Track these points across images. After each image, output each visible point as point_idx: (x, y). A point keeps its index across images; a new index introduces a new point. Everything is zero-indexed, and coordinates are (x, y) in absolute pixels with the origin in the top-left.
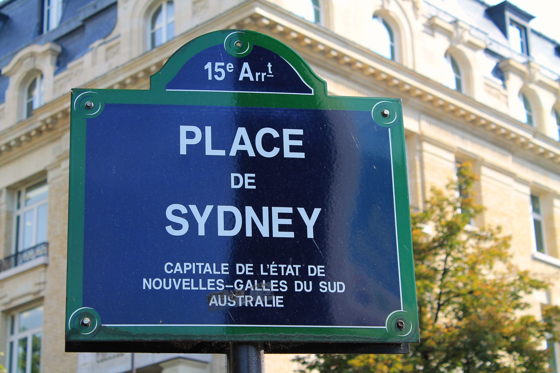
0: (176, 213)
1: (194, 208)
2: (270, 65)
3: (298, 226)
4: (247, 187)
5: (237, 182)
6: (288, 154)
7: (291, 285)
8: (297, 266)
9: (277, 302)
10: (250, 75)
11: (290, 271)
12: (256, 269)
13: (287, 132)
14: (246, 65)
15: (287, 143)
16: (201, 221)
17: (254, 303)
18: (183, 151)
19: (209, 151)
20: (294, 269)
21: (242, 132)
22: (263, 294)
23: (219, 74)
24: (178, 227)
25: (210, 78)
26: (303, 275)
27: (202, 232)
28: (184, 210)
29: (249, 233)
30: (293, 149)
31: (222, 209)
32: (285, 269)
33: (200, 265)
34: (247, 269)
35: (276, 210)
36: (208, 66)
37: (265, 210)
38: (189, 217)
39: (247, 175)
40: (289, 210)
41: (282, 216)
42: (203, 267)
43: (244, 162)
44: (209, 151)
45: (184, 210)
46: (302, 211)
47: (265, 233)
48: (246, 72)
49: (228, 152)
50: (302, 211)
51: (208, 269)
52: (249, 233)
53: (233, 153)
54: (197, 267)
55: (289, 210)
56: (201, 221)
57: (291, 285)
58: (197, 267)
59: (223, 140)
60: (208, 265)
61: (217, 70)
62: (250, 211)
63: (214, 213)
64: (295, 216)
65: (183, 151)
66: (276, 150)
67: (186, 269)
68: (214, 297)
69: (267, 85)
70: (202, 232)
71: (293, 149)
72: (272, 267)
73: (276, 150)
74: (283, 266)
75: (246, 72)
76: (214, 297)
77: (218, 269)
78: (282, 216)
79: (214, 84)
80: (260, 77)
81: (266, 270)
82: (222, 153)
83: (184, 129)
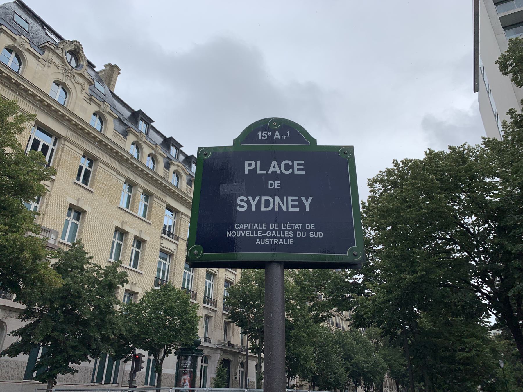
0: (242, 200)
1: (250, 198)
2: (288, 132)
3: (301, 205)
4: (276, 187)
5: (271, 186)
6: (296, 172)
8: (300, 225)
9: (290, 242)
10: (279, 137)
11: (297, 227)
12: (280, 226)
13: (296, 162)
14: (277, 132)
15: (296, 167)
16: (254, 204)
17: (278, 242)
18: (246, 172)
19: (259, 172)
20: (299, 226)
21: (274, 163)
22: (283, 238)
23: (264, 137)
24: (242, 207)
25: (260, 138)
26: (303, 229)
27: (254, 209)
28: (245, 199)
29: (277, 209)
30: (299, 170)
31: (264, 198)
32: (295, 226)
33: (252, 224)
34: (275, 226)
35: (290, 198)
36: (260, 133)
37: (285, 198)
38: (248, 202)
39: (276, 182)
40: (297, 198)
41: (293, 201)
42: (254, 226)
43: (275, 176)
44: (259, 172)
45: (245, 199)
46: (303, 198)
47: (285, 209)
48: (277, 135)
49: (267, 172)
50: (303, 198)
51: (256, 226)
52: (277, 209)
53: (270, 172)
54: (251, 226)
55: (297, 198)
56: (254, 204)
58: (251, 226)
59: (265, 166)
60: (256, 224)
61: (263, 135)
62: (277, 199)
63: (260, 200)
64: (300, 201)
65: (246, 172)
66: (291, 171)
67: (245, 226)
68: (258, 240)
69: (287, 141)
70: (254, 209)
71: (299, 170)
72: (288, 225)
73: (291, 171)
74: (293, 225)
75: (277, 135)
76: (258, 240)
77: (261, 226)
78: (293, 201)
79: (262, 141)
80: (283, 137)
81: (285, 226)
82: (265, 172)
83: (247, 162)
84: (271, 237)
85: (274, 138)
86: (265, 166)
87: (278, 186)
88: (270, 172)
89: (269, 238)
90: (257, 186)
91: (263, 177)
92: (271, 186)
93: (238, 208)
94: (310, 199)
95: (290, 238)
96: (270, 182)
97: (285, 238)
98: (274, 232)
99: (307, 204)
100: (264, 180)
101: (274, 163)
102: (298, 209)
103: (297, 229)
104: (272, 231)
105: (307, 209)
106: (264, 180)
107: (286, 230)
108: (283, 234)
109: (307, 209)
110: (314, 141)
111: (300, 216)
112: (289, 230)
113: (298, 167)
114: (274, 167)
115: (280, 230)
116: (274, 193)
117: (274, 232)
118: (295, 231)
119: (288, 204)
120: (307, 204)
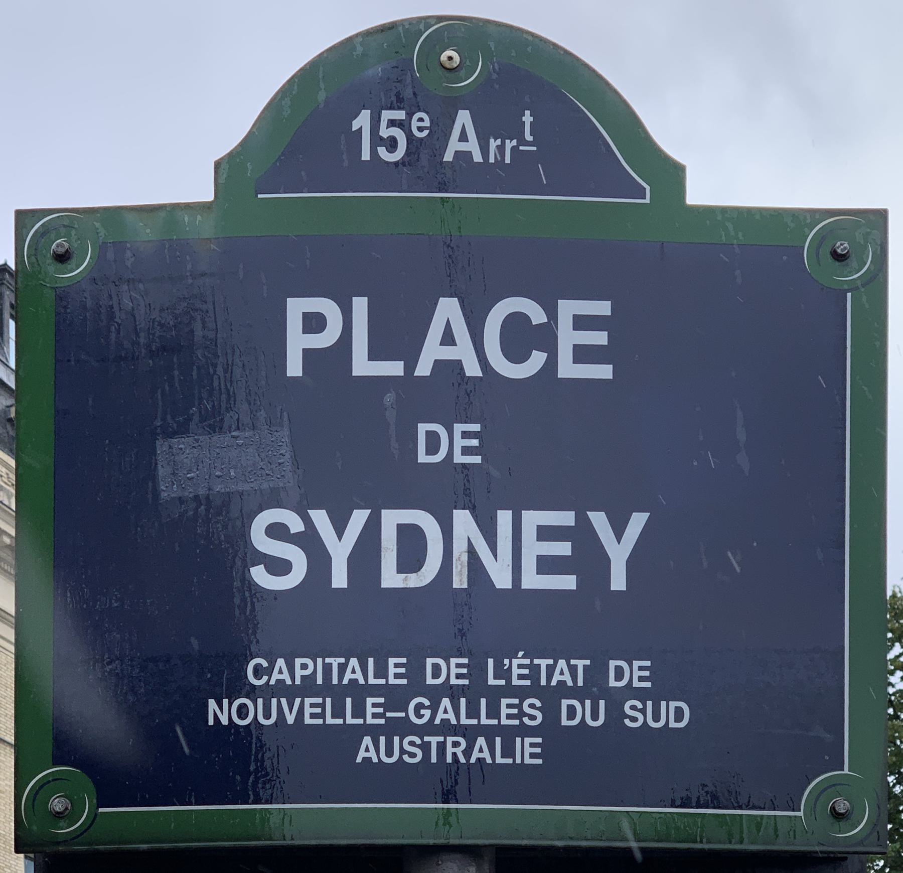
0: (277, 531)
1: (320, 518)
2: (528, 118)
3: (588, 558)
4: (459, 458)
5: (432, 449)
6: (568, 369)
7: (551, 711)
8: (580, 664)
10: (473, 146)
11: (562, 674)
12: (476, 671)
13: (567, 309)
15: (568, 338)
16: (340, 551)
18: (294, 368)
19: (362, 365)
20: (573, 670)
21: (448, 310)
22: (489, 733)
24: (280, 567)
26: (594, 687)
27: (340, 579)
28: (296, 525)
30: (582, 354)
32: (551, 670)
33: (335, 662)
35: (532, 519)
37: (504, 518)
38: (309, 541)
39: (459, 428)
40: (567, 518)
41: (545, 533)
43: (452, 392)
44: (362, 365)
45: (296, 525)
46: (599, 520)
48: (463, 137)
49: (410, 367)
50: (599, 520)
53: (423, 369)
54: (327, 668)
55: (567, 518)
56: (340, 551)
57: (551, 711)
58: (327, 668)
59: (397, 335)
63: (373, 528)
64: (582, 535)
65: (294, 368)
66: (538, 359)
67: (299, 673)
69: (516, 175)
70: (340, 579)
71: (582, 354)
72: (517, 665)
73: (538, 359)
74: (543, 663)
75: (464, 139)
78: (545, 533)
80: (501, 149)
81: (503, 673)
82: (394, 368)
83: (297, 308)
84: (430, 728)
85: (448, 157)
86: (397, 335)
87: (466, 451)
88: (423, 369)
89: (421, 731)
90: (354, 447)
91: (389, 399)
92: (432, 449)
93: (259, 575)
94: (638, 521)
95: (525, 731)
96: (423, 428)
97: (500, 730)
98: (446, 702)
99: (619, 554)
100: (391, 415)
101: (448, 310)
102: (569, 582)
103: (562, 683)
104: (435, 695)
105: (618, 581)
106: (391, 415)
107: (509, 690)
108: (493, 712)
109: (618, 581)
110: (671, 174)
111: (579, 621)
112: (522, 693)
113: (577, 338)
114: (449, 338)
115: (473, 691)
116: (446, 491)
117: (446, 702)
118: (551, 697)
119: (519, 552)
120: (619, 554)
